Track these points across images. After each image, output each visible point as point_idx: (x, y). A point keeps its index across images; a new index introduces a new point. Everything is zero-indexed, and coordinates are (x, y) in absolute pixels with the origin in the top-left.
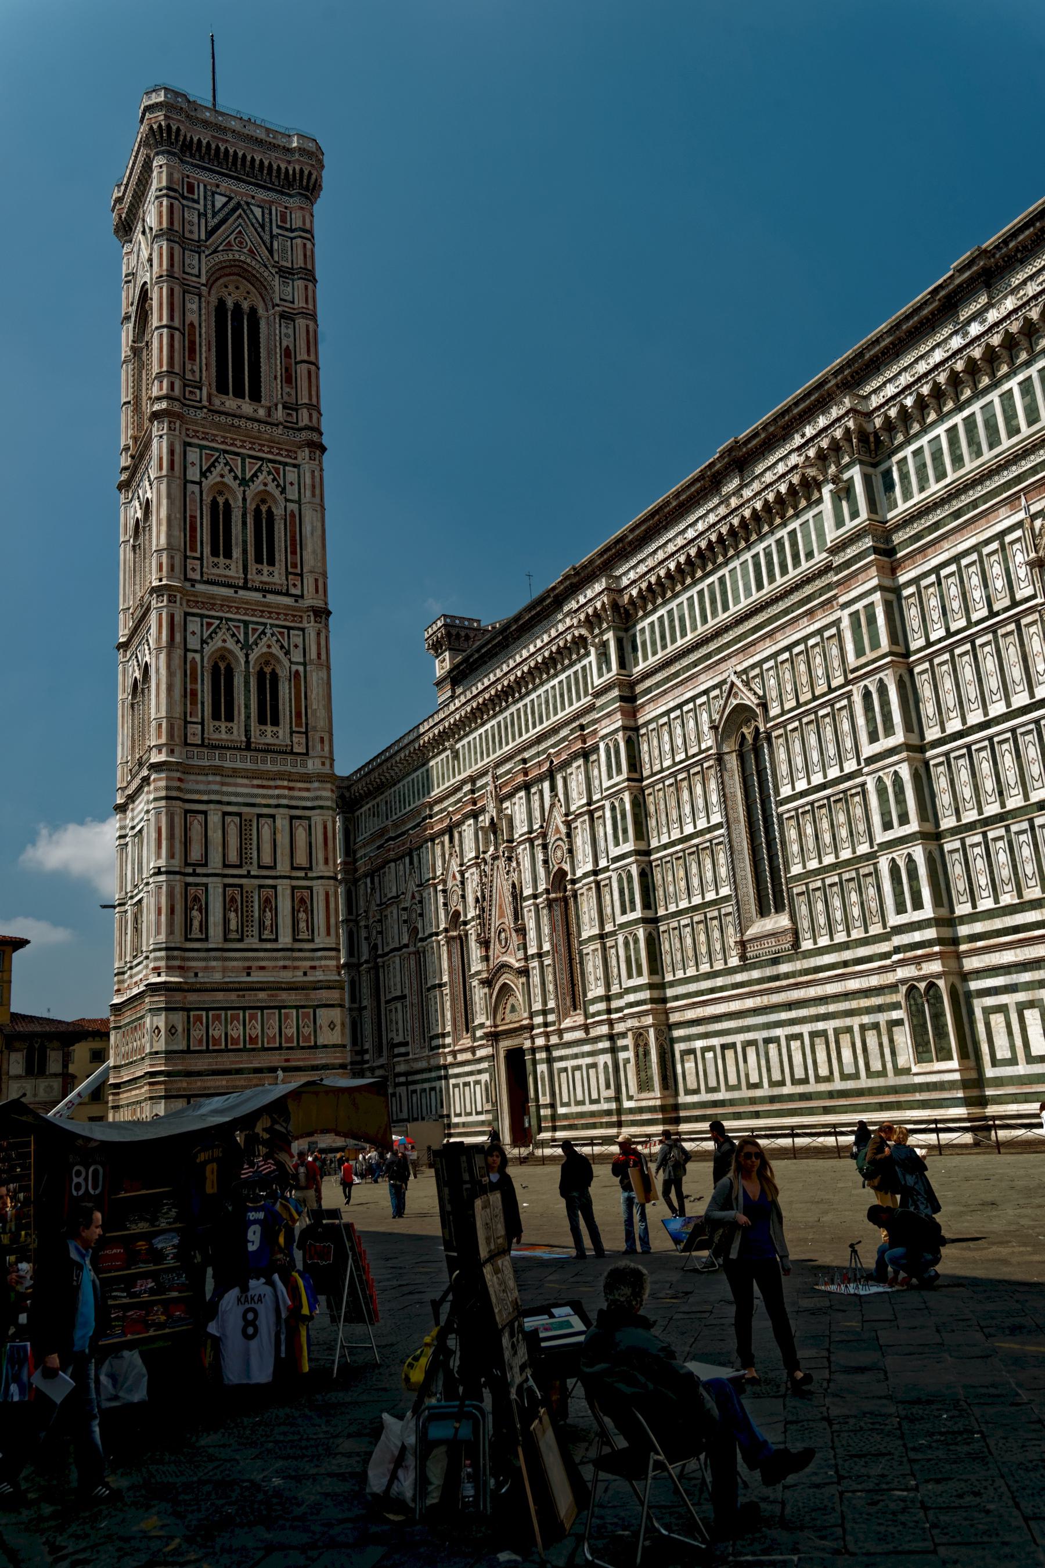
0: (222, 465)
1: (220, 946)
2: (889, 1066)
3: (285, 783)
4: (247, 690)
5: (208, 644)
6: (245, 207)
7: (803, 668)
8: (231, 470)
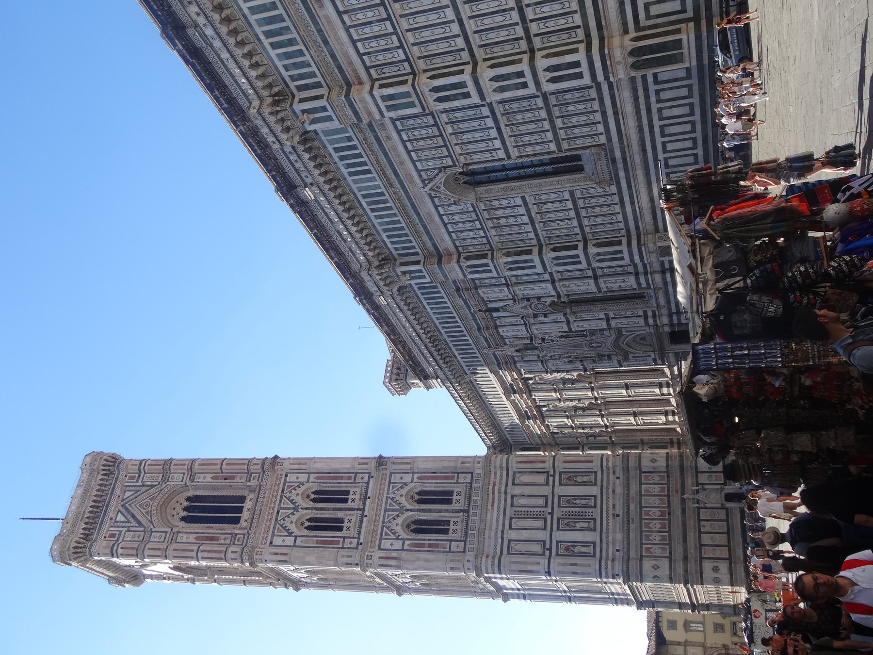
1: (599, 534)
2: (685, 83)
3: (491, 487)
4: (430, 511)
6: (125, 502)
7: (421, 143)
8: (288, 516)
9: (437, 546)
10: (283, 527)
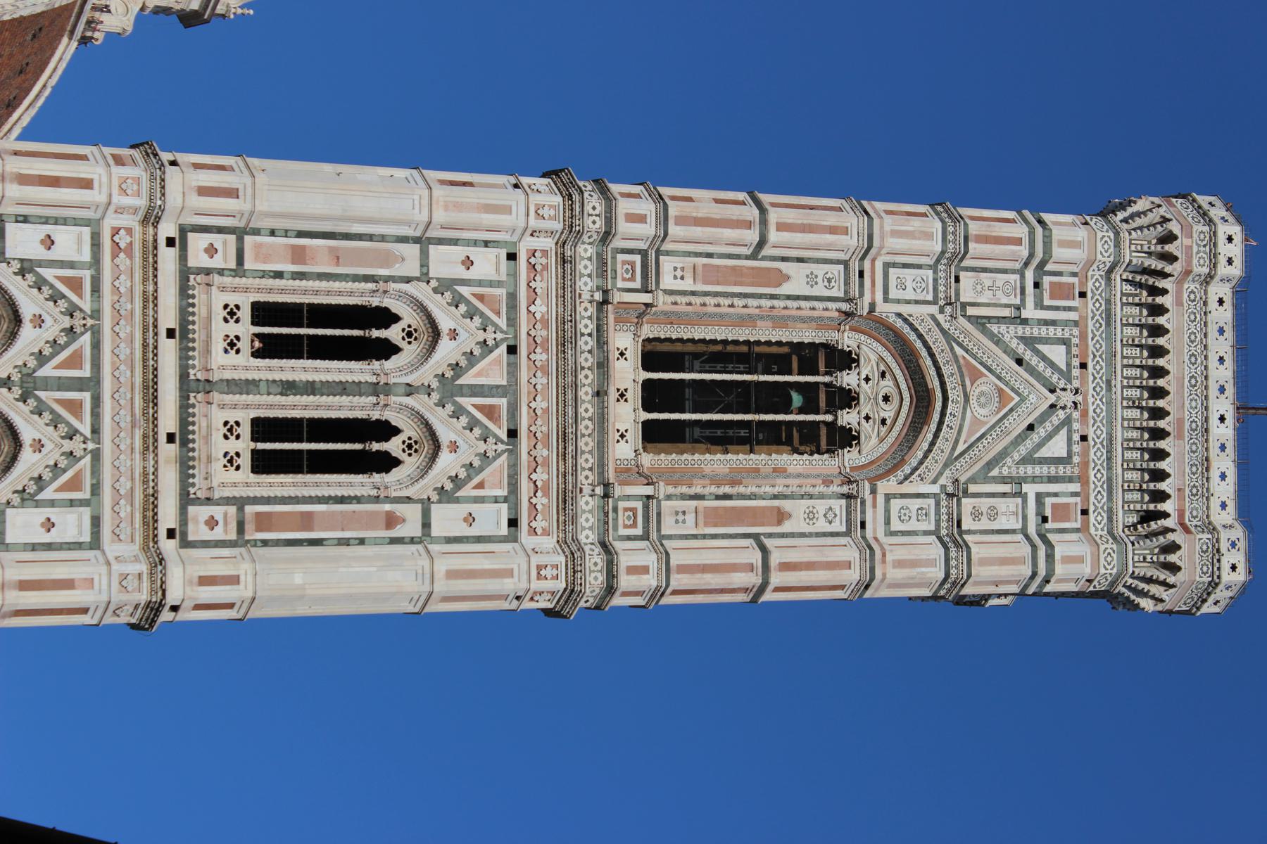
0: (481, 336)
5: (22, 272)
10: (482, 315)
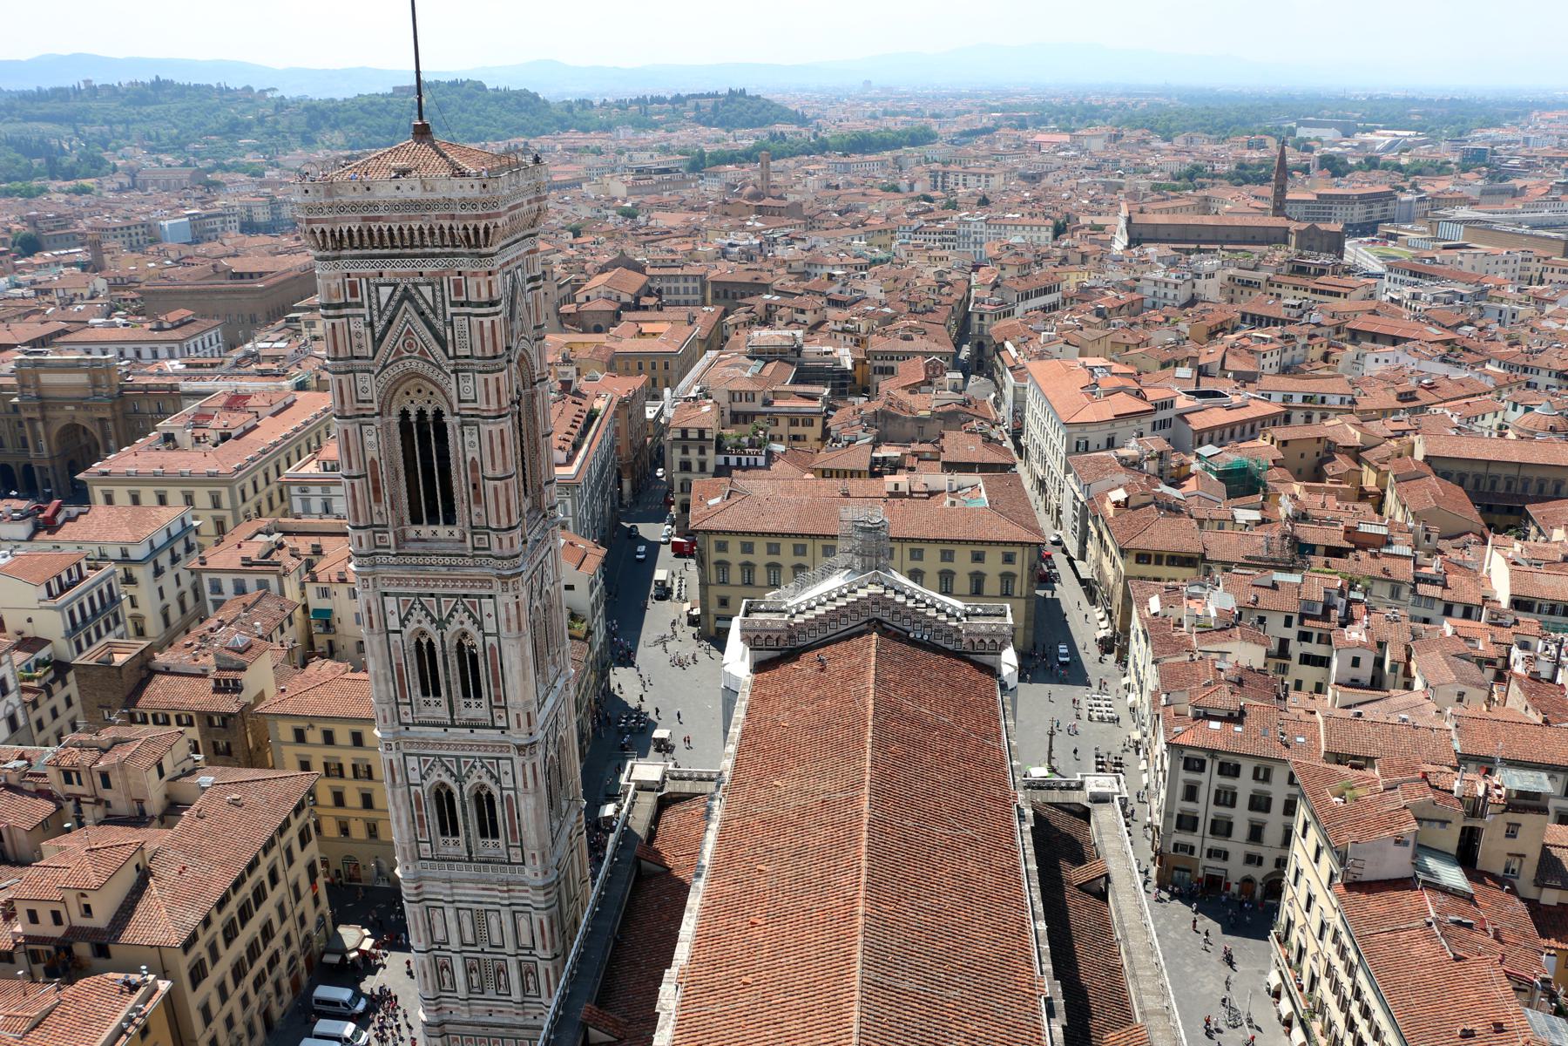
6: (413, 292)
9: (421, 825)
